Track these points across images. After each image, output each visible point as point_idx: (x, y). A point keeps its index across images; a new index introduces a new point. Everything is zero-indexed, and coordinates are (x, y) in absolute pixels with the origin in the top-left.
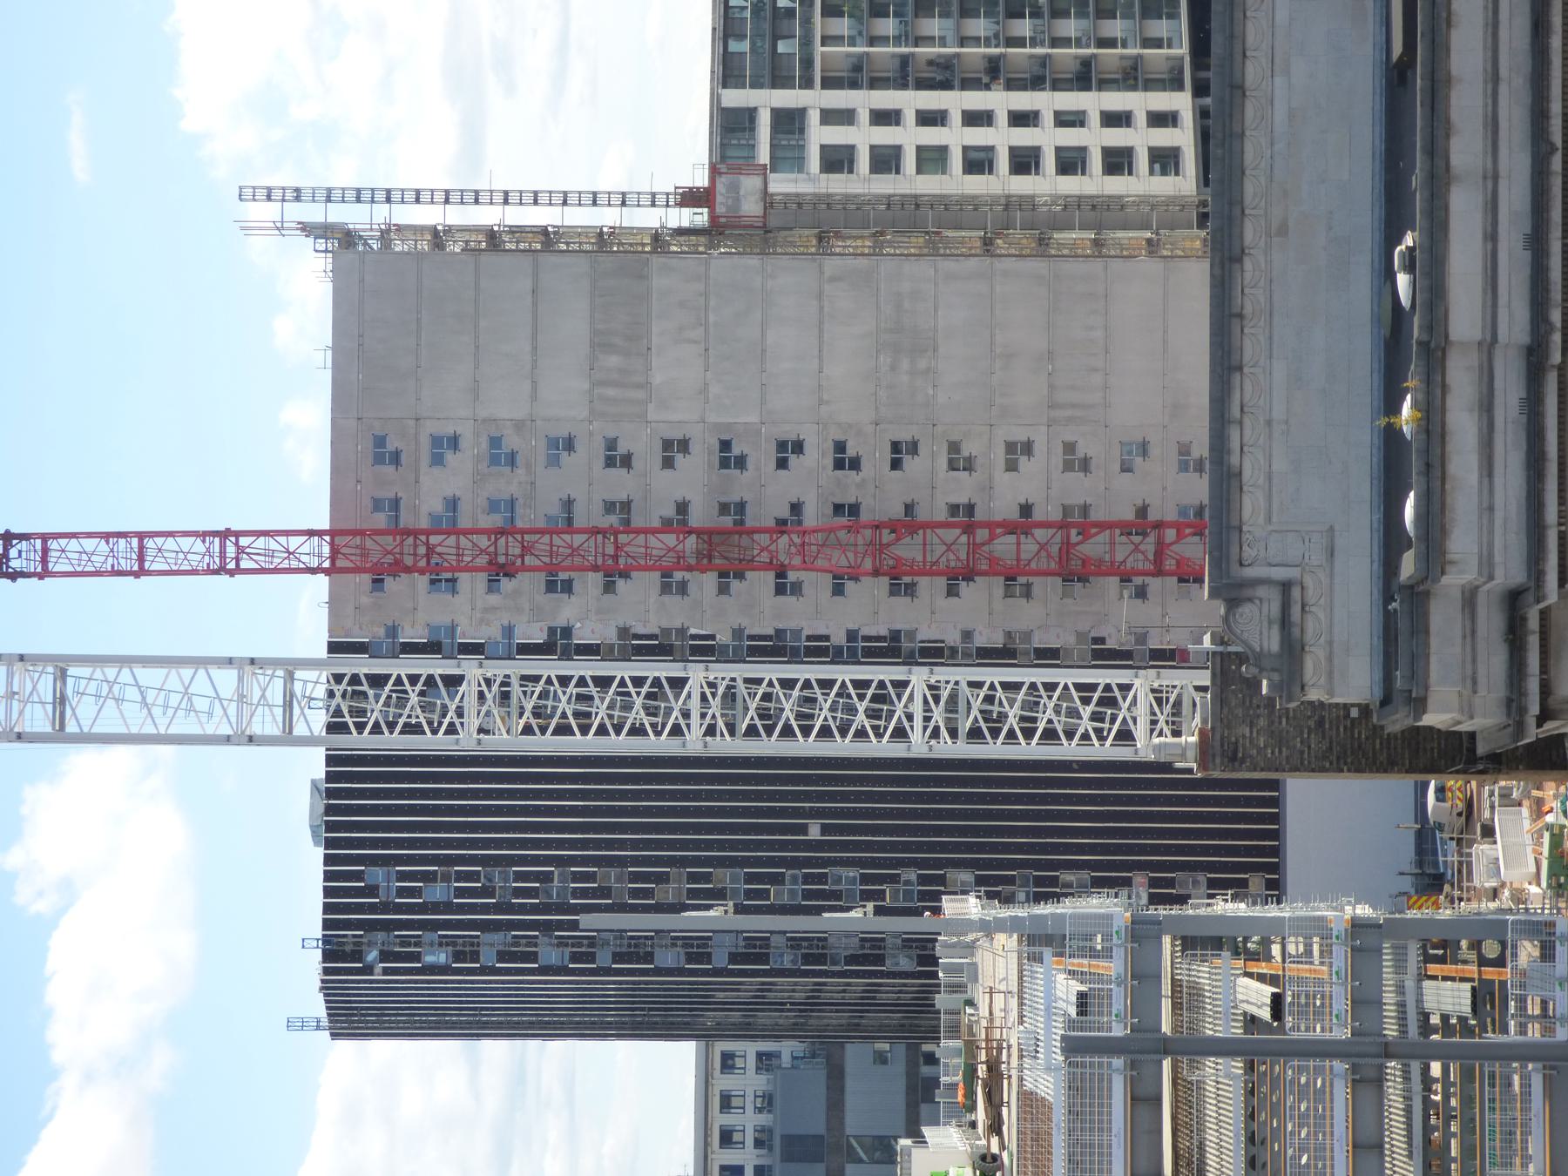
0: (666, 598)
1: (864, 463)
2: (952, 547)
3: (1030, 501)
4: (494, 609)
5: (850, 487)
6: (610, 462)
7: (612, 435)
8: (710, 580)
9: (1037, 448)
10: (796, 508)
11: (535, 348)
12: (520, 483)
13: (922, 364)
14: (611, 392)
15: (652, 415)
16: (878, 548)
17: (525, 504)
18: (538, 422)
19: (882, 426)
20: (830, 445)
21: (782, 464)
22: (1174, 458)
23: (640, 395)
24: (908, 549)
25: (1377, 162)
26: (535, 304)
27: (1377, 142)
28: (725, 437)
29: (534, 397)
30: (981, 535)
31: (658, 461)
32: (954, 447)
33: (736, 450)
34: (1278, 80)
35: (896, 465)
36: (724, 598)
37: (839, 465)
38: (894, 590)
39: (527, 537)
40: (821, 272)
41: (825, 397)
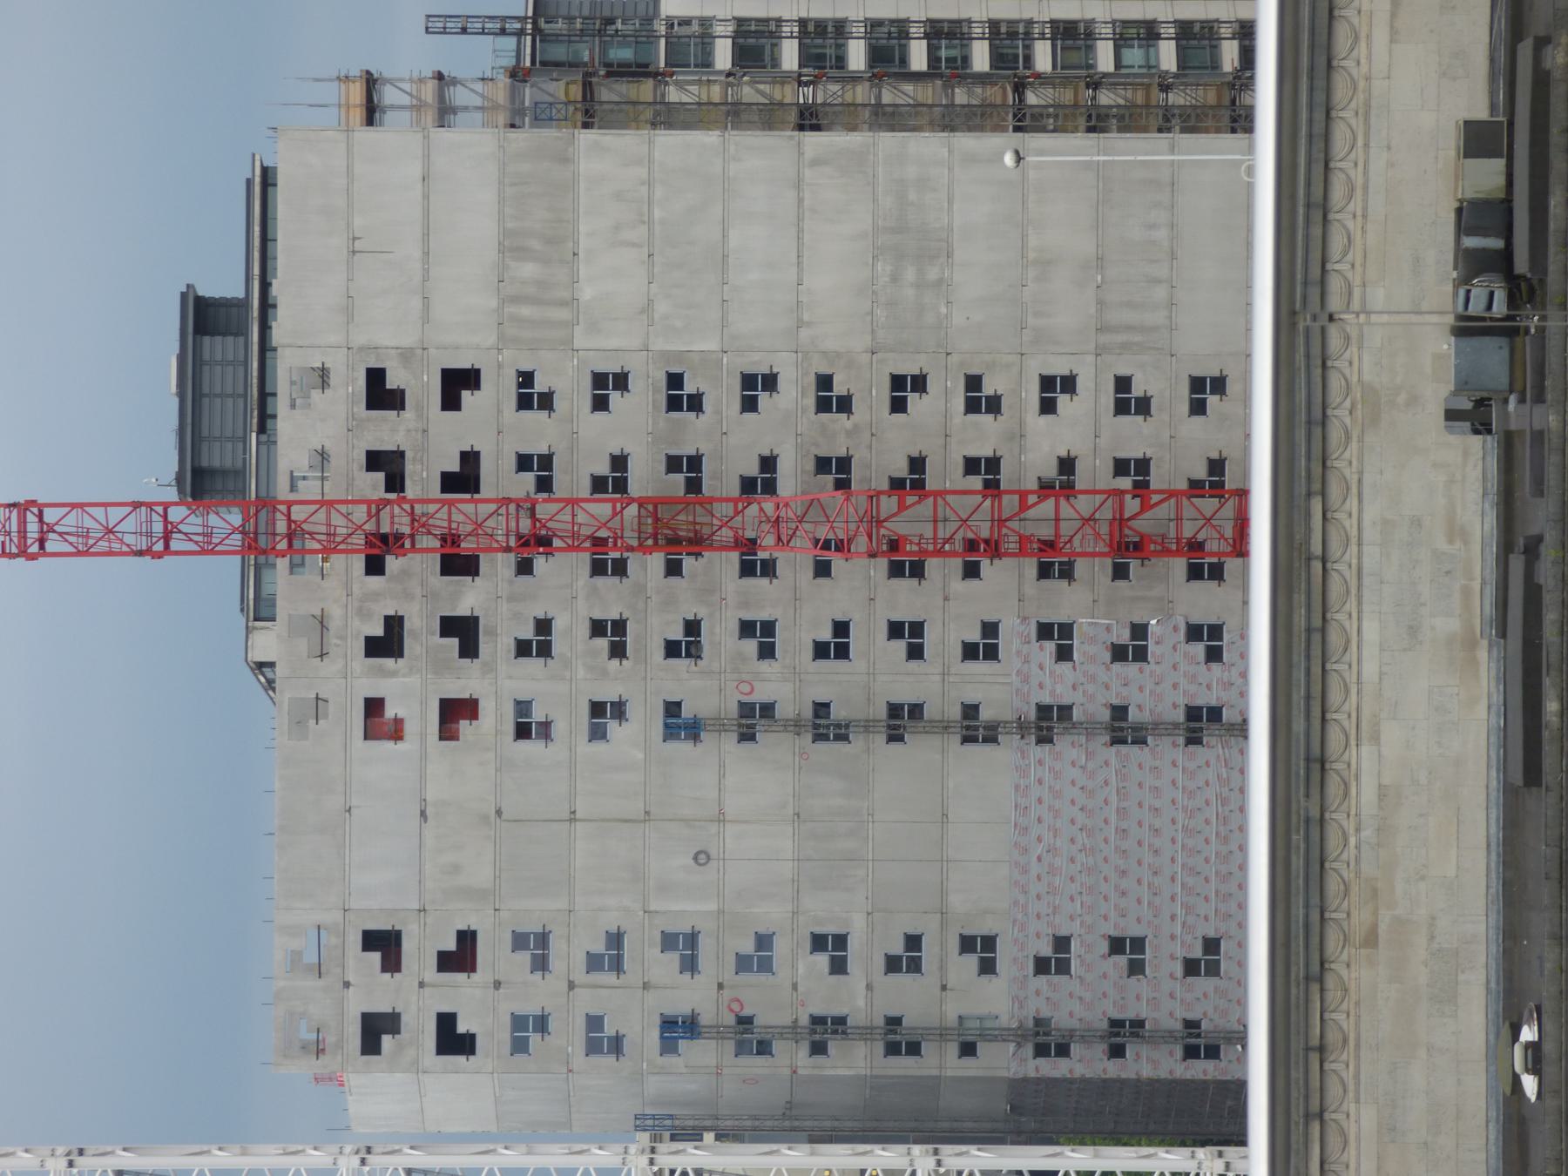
0: (600, 581)
1: (856, 404)
2: (969, 523)
3: (1073, 454)
4: (376, 596)
5: (837, 436)
6: (524, 403)
7: (526, 367)
8: (657, 561)
9: (1081, 384)
10: (768, 463)
11: (426, 254)
12: (409, 431)
14: (526, 311)
17: (414, 459)
18: (432, 351)
19: (880, 355)
20: (812, 379)
21: (750, 405)
23: (563, 314)
24: (913, 523)
25: (1494, 856)
26: (426, 196)
27: (1493, 830)
28: (675, 370)
29: (426, 317)
30: (1010, 503)
31: (587, 402)
32: (973, 382)
33: (689, 388)
34: (1365, 749)
35: (898, 406)
36: (674, 580)
37: (823, 405)
40: (800, 154)
41: (806, 317)
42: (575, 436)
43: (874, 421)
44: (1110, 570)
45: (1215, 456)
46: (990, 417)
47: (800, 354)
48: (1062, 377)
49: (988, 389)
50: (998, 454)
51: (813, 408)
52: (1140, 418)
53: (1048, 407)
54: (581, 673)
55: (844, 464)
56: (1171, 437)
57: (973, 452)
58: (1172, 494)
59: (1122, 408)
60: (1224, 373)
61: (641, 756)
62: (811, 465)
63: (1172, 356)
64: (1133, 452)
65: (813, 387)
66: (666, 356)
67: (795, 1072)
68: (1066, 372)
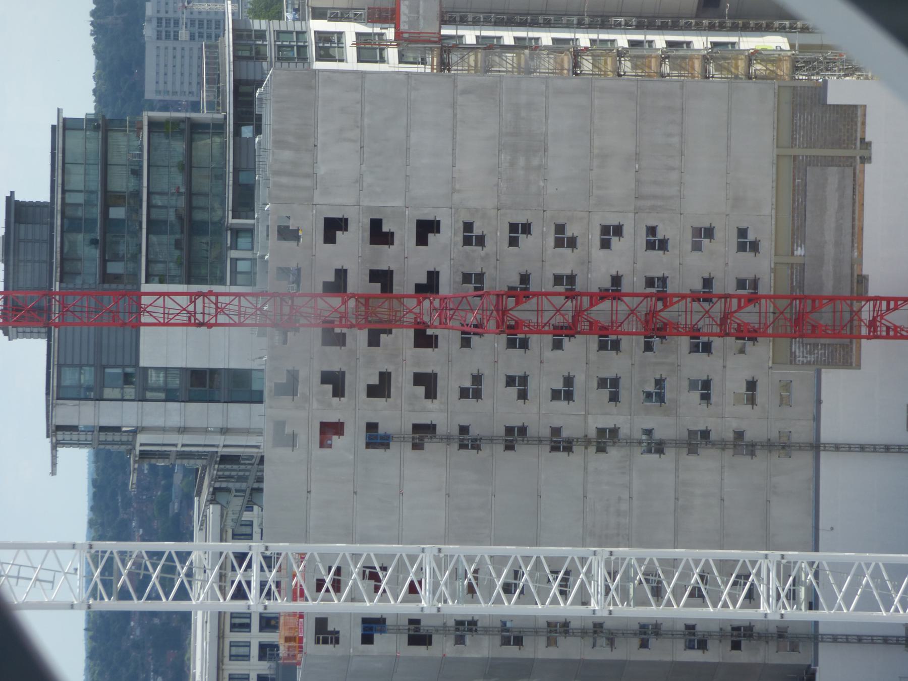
3: (620, 274)
9: (626, 230)
13: (535, 162)
14: (284, 180)
15: (316, 200)
16: (503, 312)
19: (502, 211)
20: (461, 225)
22: (734, 239)
23: (308, 182)
24: (525, 312)
32: (560, 229)
35: (513, 242)
36: (374, 349)
38: (511, 344)
39: (221, 299)
40: (455, 87)
41: (457, 187)
42: (314, 257)
43: (498, 252)
44: (642, 345)
45: (706, 276)
46: (570, 250)
47: (453, 209)
48: (614, 226)
49: (569, 233)
50: (574, 273)
51: (462, 244)
52: (661, 252)
53: (605, 244)
54: (315, 405)
55: (480, 277)
56: (680, 264)
57: (560, 271)
58: (683, 297)
59: (650, 246)
60: (713, 225)
61: (352, 457)
62: (459, 278)
63: (681, 214)
64: (657, 273)
65: (462, 230)
66: (369, 208)
67: (444, 655)
68: (616, 223)
